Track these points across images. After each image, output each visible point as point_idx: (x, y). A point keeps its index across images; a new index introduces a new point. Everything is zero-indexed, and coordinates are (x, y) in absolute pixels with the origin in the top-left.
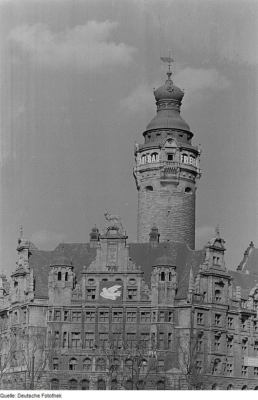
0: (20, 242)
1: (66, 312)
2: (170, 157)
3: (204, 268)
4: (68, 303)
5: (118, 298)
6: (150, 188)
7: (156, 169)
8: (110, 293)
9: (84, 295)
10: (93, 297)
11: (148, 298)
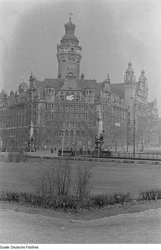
0: (31, 77)
1: (52, 105)
2: (72, 49)
3: (105, 90)
4: (53, 101)
5: (73, 100)
6: (64, 61)
7: (67, 54)
8: (70, 98)
9: (59, 98)
10: (63, 99)
11: (84, 100)
